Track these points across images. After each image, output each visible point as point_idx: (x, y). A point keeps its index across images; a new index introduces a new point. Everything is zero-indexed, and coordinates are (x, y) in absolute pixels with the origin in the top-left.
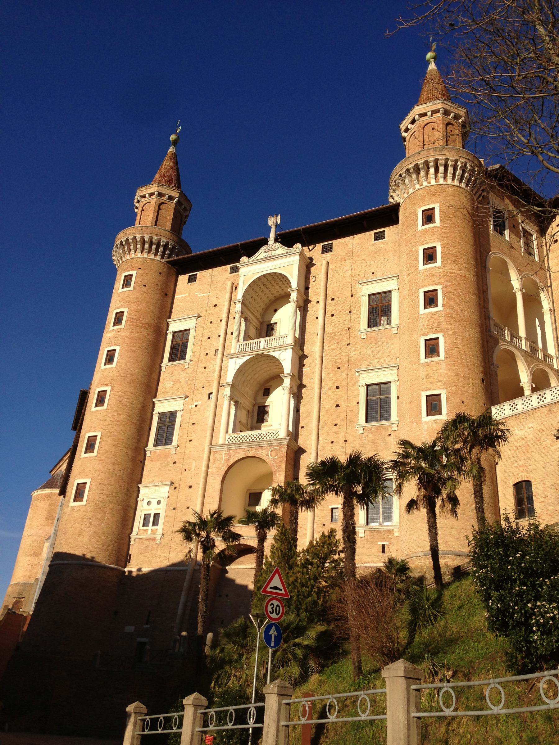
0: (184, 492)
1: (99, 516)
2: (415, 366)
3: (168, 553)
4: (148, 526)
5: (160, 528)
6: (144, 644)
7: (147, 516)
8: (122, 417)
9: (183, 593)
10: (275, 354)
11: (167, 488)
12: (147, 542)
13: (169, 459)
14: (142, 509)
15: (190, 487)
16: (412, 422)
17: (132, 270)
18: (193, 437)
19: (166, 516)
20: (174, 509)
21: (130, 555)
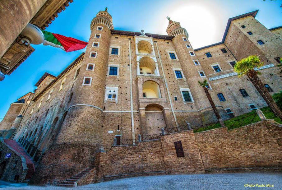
0: (124, 90)
1: (96, 90)
2: (194, 66)
3: (121, 107)
4: (111, 98)
5: (116, 99)
6: (119, 137)
7: (110, 96)
8: (102, 62)
9: (133, 119)
10: (152, 58)
11: (117, 87)
12: (112, 103)
13: (116, 79)
14: (107, 93)
15: (126, 88)
16: (198, 77)
17: (101, 26)
18: (125, 74)
19: (118, 96)
20: (121, 93)
21: (104, 107)
